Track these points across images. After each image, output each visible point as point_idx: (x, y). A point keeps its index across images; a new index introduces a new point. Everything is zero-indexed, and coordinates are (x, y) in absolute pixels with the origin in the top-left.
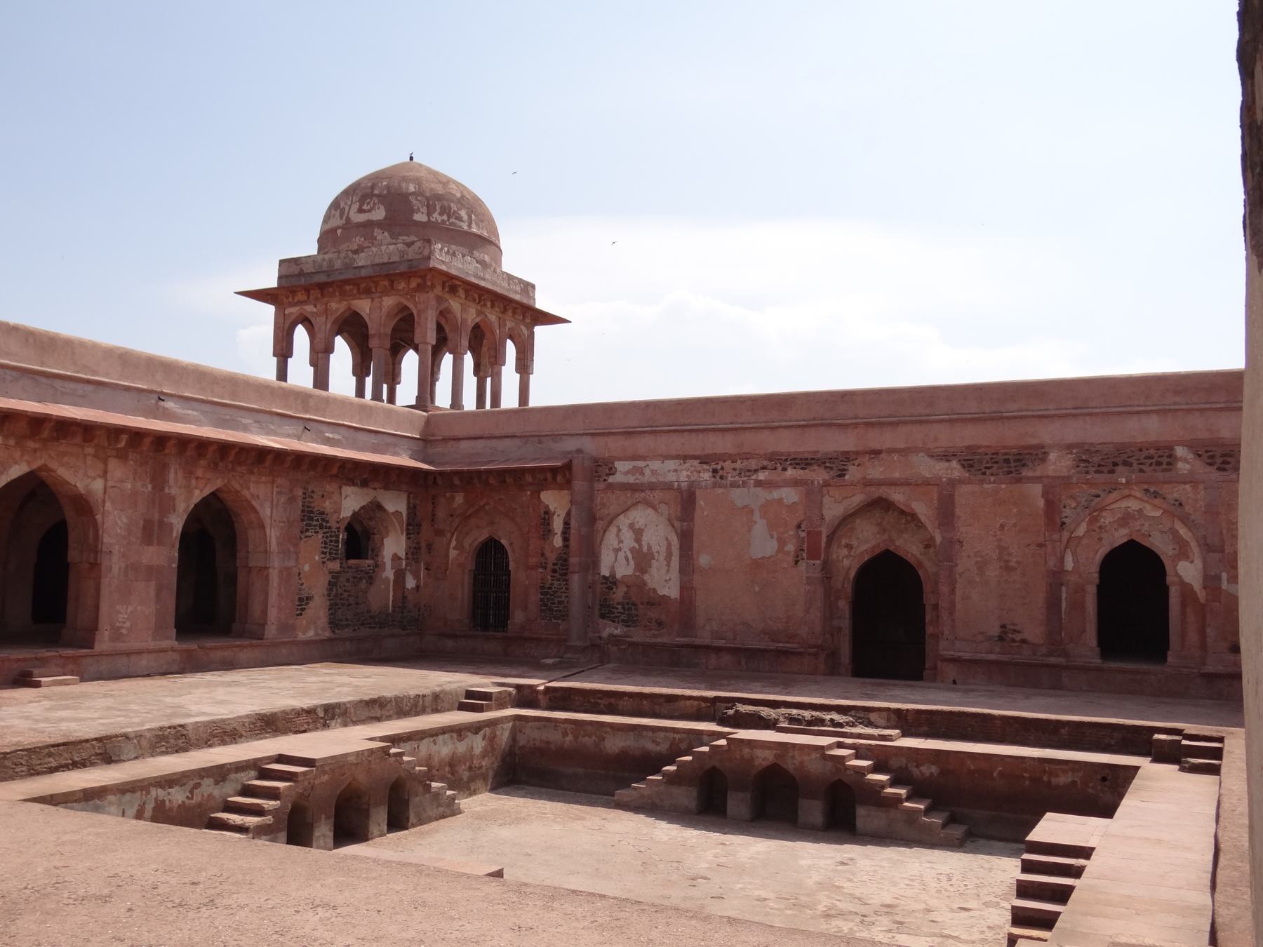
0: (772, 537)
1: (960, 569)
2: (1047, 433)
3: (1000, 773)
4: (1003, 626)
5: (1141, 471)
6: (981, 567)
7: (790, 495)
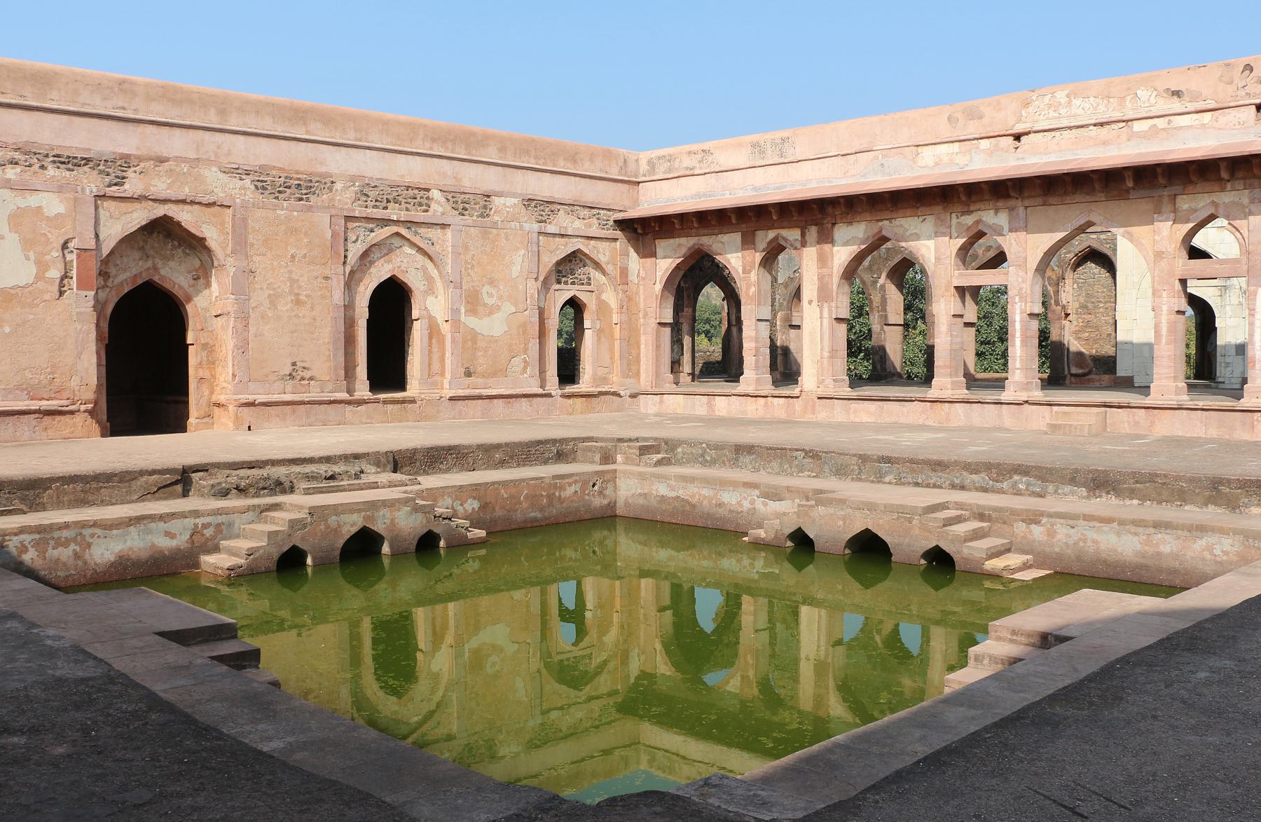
0: (27, 258)
1: (253, 303)
2: (336, 163)
3: (527, 497)
4: (294, 364)
5: (407, 210)
6: (273, 300)
7: (53, 205)
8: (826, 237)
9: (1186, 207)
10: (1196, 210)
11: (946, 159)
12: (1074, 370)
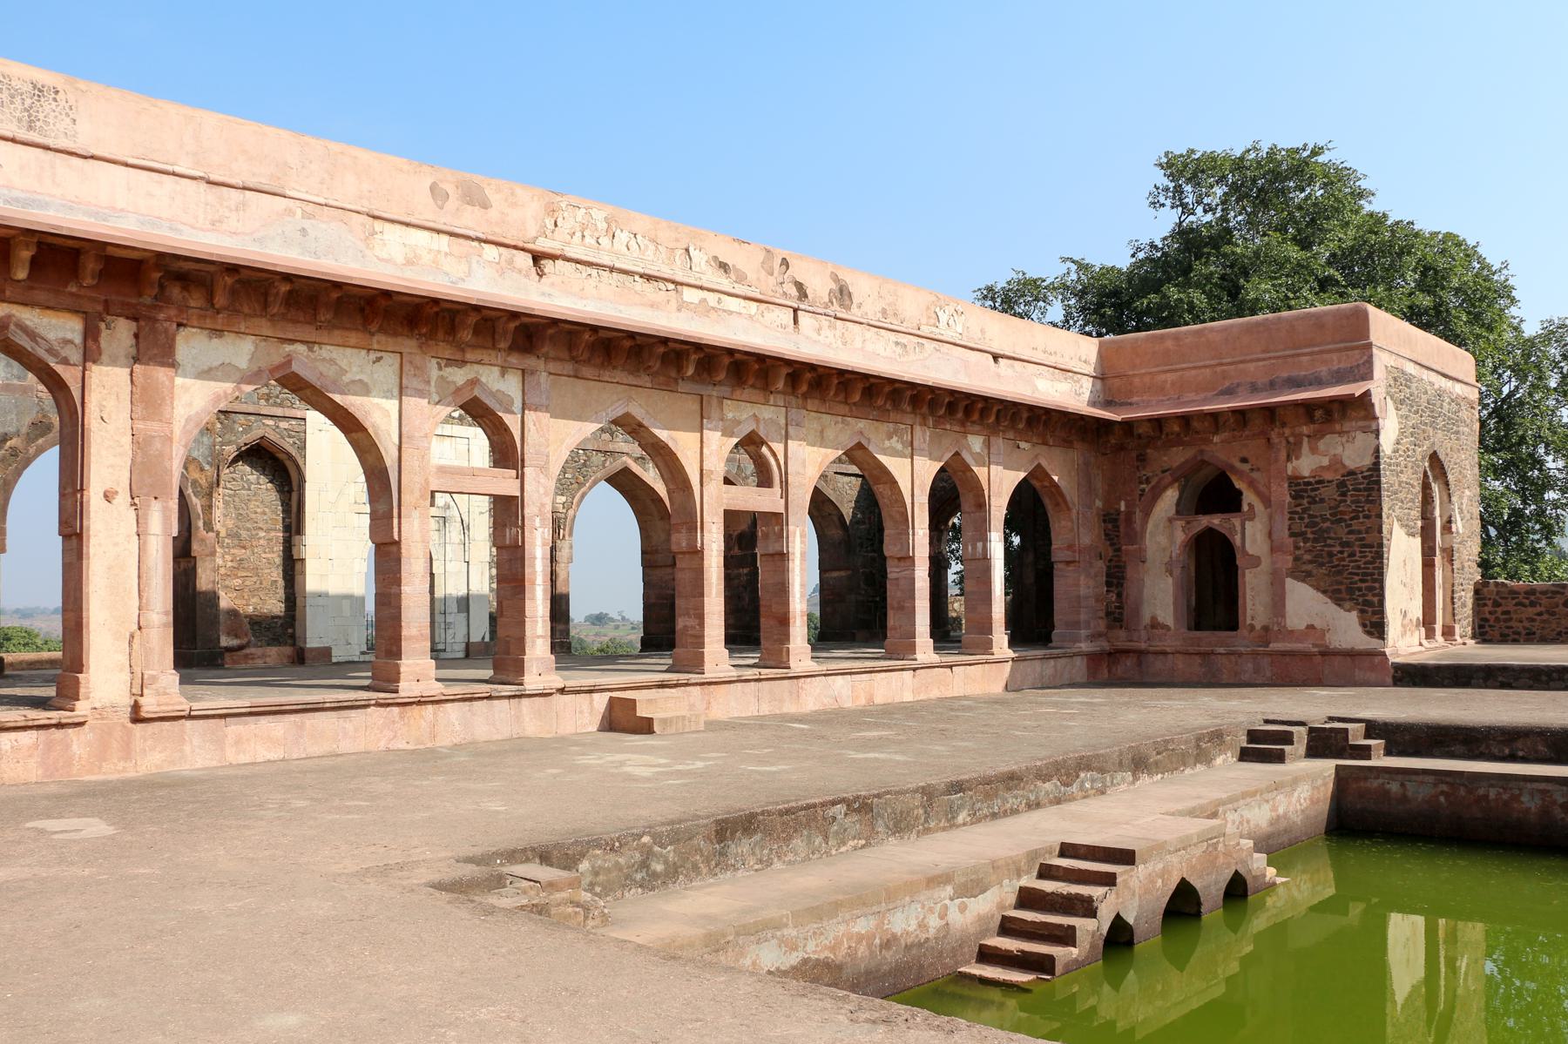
8: (153, 349)
9: (730, 415)
10: (739, 423)
11: (426, 258)
12: (225, 641)
